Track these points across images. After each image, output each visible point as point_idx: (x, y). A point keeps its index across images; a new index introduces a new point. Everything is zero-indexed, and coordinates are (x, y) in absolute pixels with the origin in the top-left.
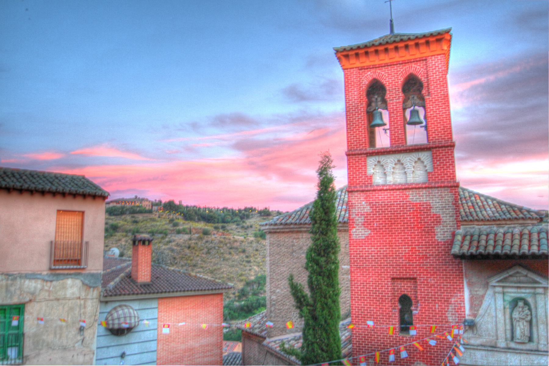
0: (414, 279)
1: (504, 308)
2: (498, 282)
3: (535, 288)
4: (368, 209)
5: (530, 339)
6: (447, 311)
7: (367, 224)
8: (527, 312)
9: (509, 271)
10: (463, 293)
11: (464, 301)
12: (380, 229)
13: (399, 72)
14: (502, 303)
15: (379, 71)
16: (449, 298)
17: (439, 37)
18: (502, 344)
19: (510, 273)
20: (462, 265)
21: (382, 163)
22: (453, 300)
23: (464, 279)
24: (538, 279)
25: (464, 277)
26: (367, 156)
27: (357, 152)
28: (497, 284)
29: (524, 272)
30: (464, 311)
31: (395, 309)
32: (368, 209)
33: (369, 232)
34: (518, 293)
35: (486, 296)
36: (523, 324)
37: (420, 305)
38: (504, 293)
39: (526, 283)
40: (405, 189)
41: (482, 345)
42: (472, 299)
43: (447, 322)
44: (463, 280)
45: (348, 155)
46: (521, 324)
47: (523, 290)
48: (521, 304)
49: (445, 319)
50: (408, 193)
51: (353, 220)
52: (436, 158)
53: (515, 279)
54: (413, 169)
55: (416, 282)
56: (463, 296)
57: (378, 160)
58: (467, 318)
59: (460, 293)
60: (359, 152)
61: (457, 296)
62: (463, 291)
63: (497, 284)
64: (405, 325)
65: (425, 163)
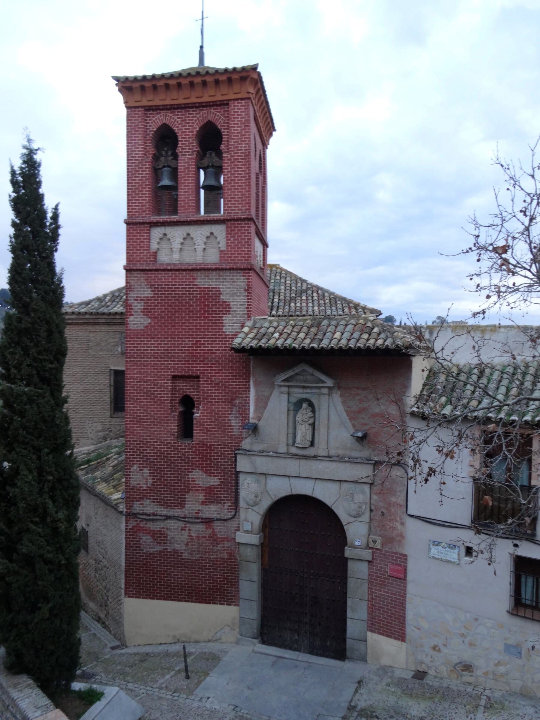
0: (198, 377)
1: (288, 410)
2: (284, 381)
3: (320, 388)
4: (148, 293)
5: (312, 444)
6: (230, 414)
7: (146, 312)
8: (310, 414)
9: (295, 369)
10: (249, 394)
11: (249, 403)
12: (161, 317)
13: (195, 118)
14: (287, 403)
15: (170, 115)
16: (234, 400)
17: (244, 74)
18: (283, 449)
19: (297, 371)
20: (250, 362)
21: (168, 237)
22: (237, 401)
23: (251, 378)
24: (323, 377)
25: (251, 375)
26: (151, 227)
27: (138, 220)
28: (282, 384)
29: (310, 370)
30: (249, 414)
31: (175, 412)
32: (148, 293)
33: (149, 321)
34: (303, 393)
35: (272, 398)
36: (305, 427)
37: (203, 407)
38: (289, 394)
39: (313, 382)
40: (193, 270)
41: (263, 451)
42: (257, 400)
43: (230, 426)
44: (249, 380)
45: (128, 223)
46: (303, 426)
47: (308, 391)
48: (305, 405)
49: (228, 423)
50: (195, 275)
51: (131, 306)
52: (231, 234)
53: (302, 377)
54: (204, 247)
55: (199, 381)
56: (248, 397)
57: (164, 232)
58: (251, 421)
59: (246, 394)
60: (141, 221)
61: (242, 397)
62: (249, 391)
63: (282, 384)
64: (186, 429)
65: (219, 239)
